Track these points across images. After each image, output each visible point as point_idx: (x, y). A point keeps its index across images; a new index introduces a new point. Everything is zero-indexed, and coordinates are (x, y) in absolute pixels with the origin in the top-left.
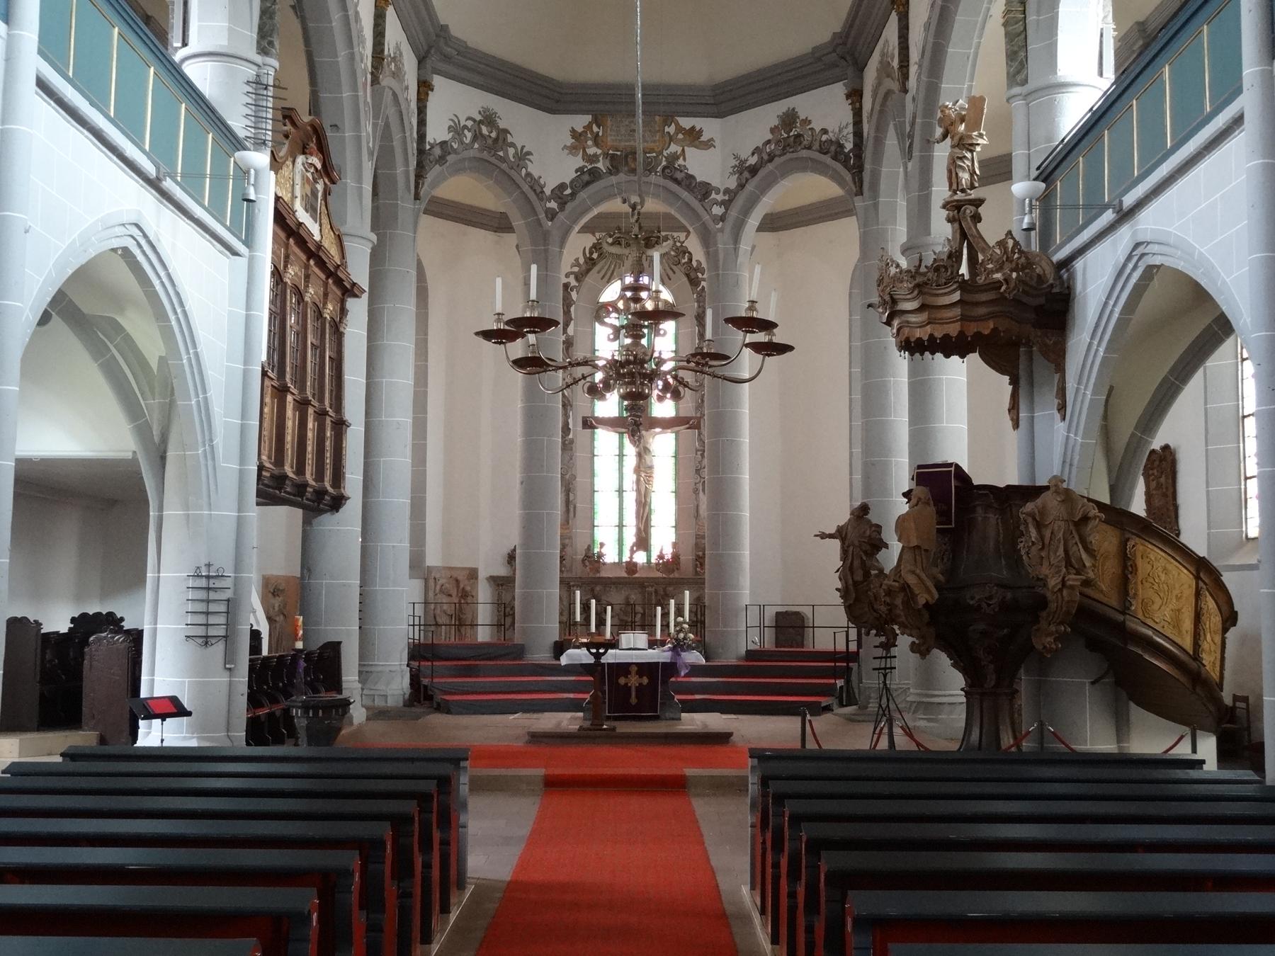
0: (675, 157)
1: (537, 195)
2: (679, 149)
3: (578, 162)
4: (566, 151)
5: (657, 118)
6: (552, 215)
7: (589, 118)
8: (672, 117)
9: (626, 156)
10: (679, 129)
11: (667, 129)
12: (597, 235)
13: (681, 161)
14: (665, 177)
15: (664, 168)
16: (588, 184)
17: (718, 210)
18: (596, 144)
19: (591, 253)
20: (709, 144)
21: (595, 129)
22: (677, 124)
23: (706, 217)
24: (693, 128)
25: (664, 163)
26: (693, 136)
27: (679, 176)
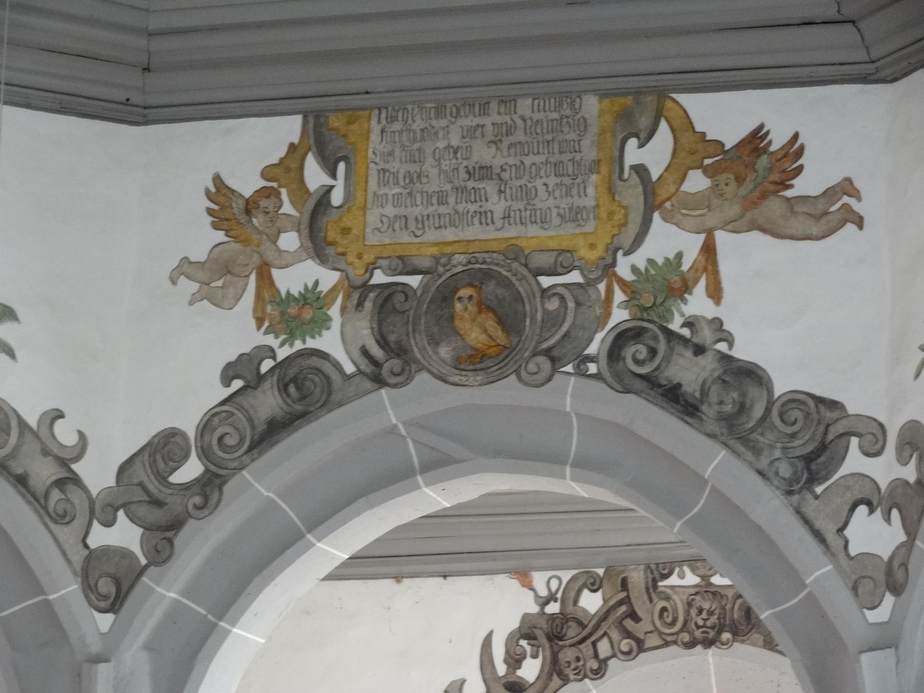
0: (671, 283)
1: (37, 500)
2: (690, 246)
3: (236, 330)
4: (189, 287)
5: (591, 105)
6: (112, 584)
7: (290, 128)
8: (663, 94)
9: (445, 297)
10: (694, 148)
11: (633, 154)
12: (539, 580)
13: (698, 303)
14: (622, 381)
15: (622, 338)
16: (275, 430)
17: (873, 535)
18: (319, 247)
19: (514, 660)
20: (834, 211)
21: (314, 176)
22: (684, 127)
23: (820, 572)
24: (756, 140)
25: (620, 315)
26: (758, 177)
27: (688, 372)
